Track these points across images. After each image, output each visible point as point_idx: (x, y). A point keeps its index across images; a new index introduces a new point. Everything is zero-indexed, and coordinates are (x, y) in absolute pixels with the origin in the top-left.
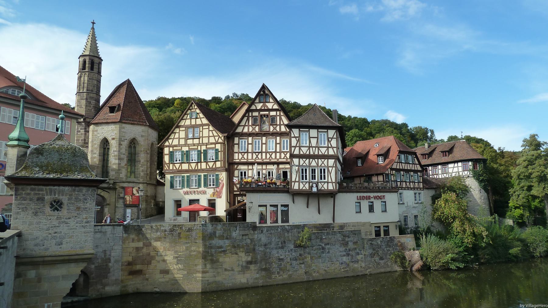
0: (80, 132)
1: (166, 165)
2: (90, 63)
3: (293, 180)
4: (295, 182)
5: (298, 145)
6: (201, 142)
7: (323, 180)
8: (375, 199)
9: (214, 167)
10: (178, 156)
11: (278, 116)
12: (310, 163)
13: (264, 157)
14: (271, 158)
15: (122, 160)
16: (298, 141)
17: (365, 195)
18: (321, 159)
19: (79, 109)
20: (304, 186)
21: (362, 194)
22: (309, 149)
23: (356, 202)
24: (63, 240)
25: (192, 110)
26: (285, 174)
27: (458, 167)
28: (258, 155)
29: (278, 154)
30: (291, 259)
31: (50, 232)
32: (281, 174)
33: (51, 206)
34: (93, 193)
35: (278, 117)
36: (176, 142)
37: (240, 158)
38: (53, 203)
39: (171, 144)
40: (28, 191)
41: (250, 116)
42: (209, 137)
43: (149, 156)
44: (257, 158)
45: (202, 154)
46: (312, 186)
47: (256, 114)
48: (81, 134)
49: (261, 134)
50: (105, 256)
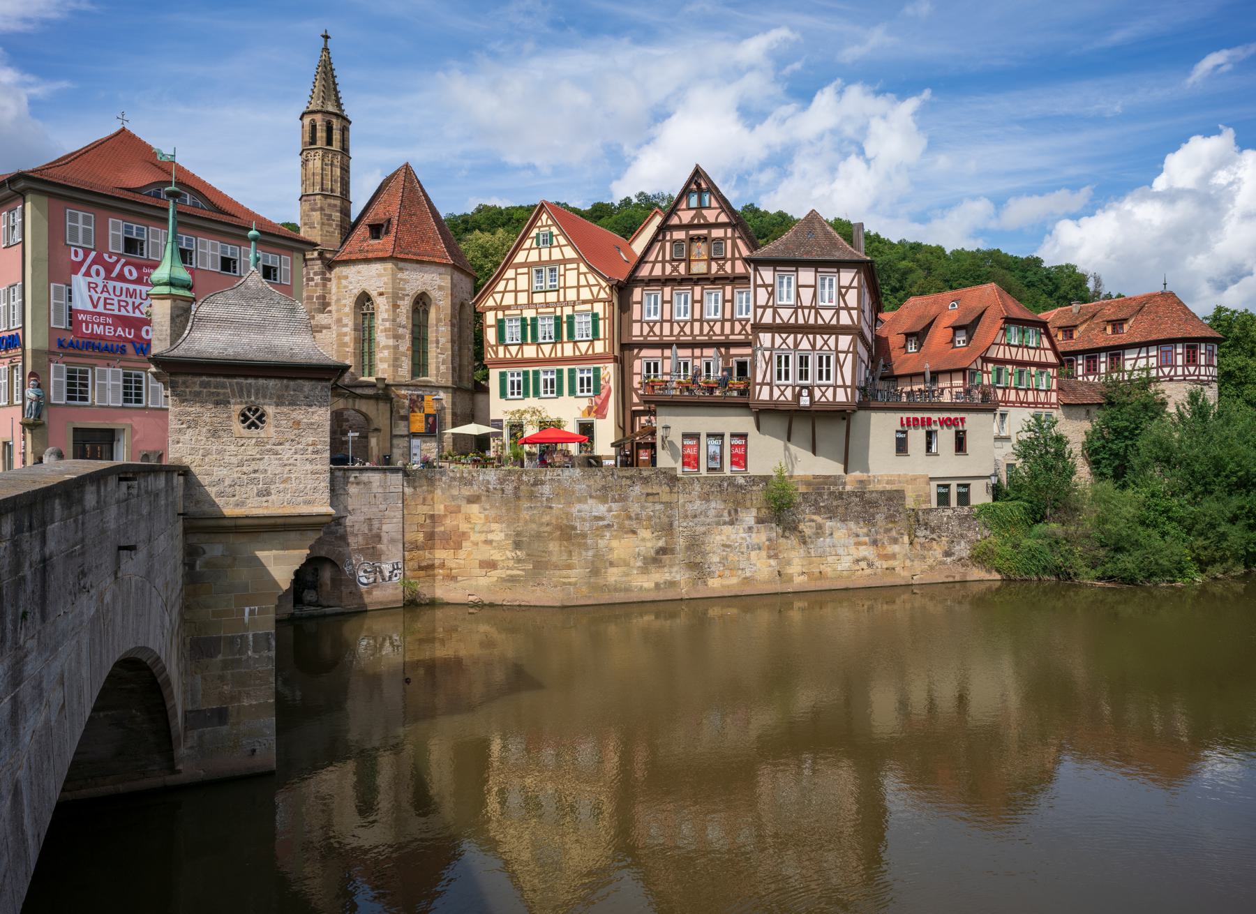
0: (312, 280)
1: (490, 349)
2: (325, 128)
3: (759, 379)
4: (762, 384)
5: (770, 303)
6: (562, 299)
7: (824, 381)
8: (941, 425)
9: (590, 352)
10: (512, 330)
11: (729, 238)
12: (796, 345)
13: (697, 331)
14: (711, 333)
16: (771, 294)
17: (919, 415)
18: (821, 334)
20: (782, 393)
21: (911, 415)
22: (796, 312)
23: (897, 431)
24: (272, 487)
25: (541, 229)
26: (742, 367)
27: (1148, 357)
28: (684, 326)
29: (728, 325)
30: (748, 547)
31: (245, 469)
32: (732, 368)
33: (242, 418)
34: (324, 393)
35: (729, 242)
36: (509, 299)
37: (645, 333)
38: (247, 413)
39: (499, 303)
40: (197, 389)
41: (668, 241)
42: (578, 287)
43: (456, 330)
44: (682, 333)
45: (565, 326)
46: (800, 394)
47: (680, 235)
48: (316, 285)
49: (691, 279)
50: (370, 530)
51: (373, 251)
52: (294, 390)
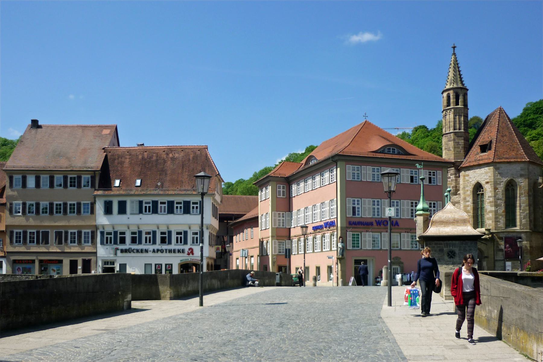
0: (450, 178)
15: (498, 206)
19: (447, 152)
40: (433, 245)
43: (531, 198)
51: (482, 160)
52: (465, 244)
